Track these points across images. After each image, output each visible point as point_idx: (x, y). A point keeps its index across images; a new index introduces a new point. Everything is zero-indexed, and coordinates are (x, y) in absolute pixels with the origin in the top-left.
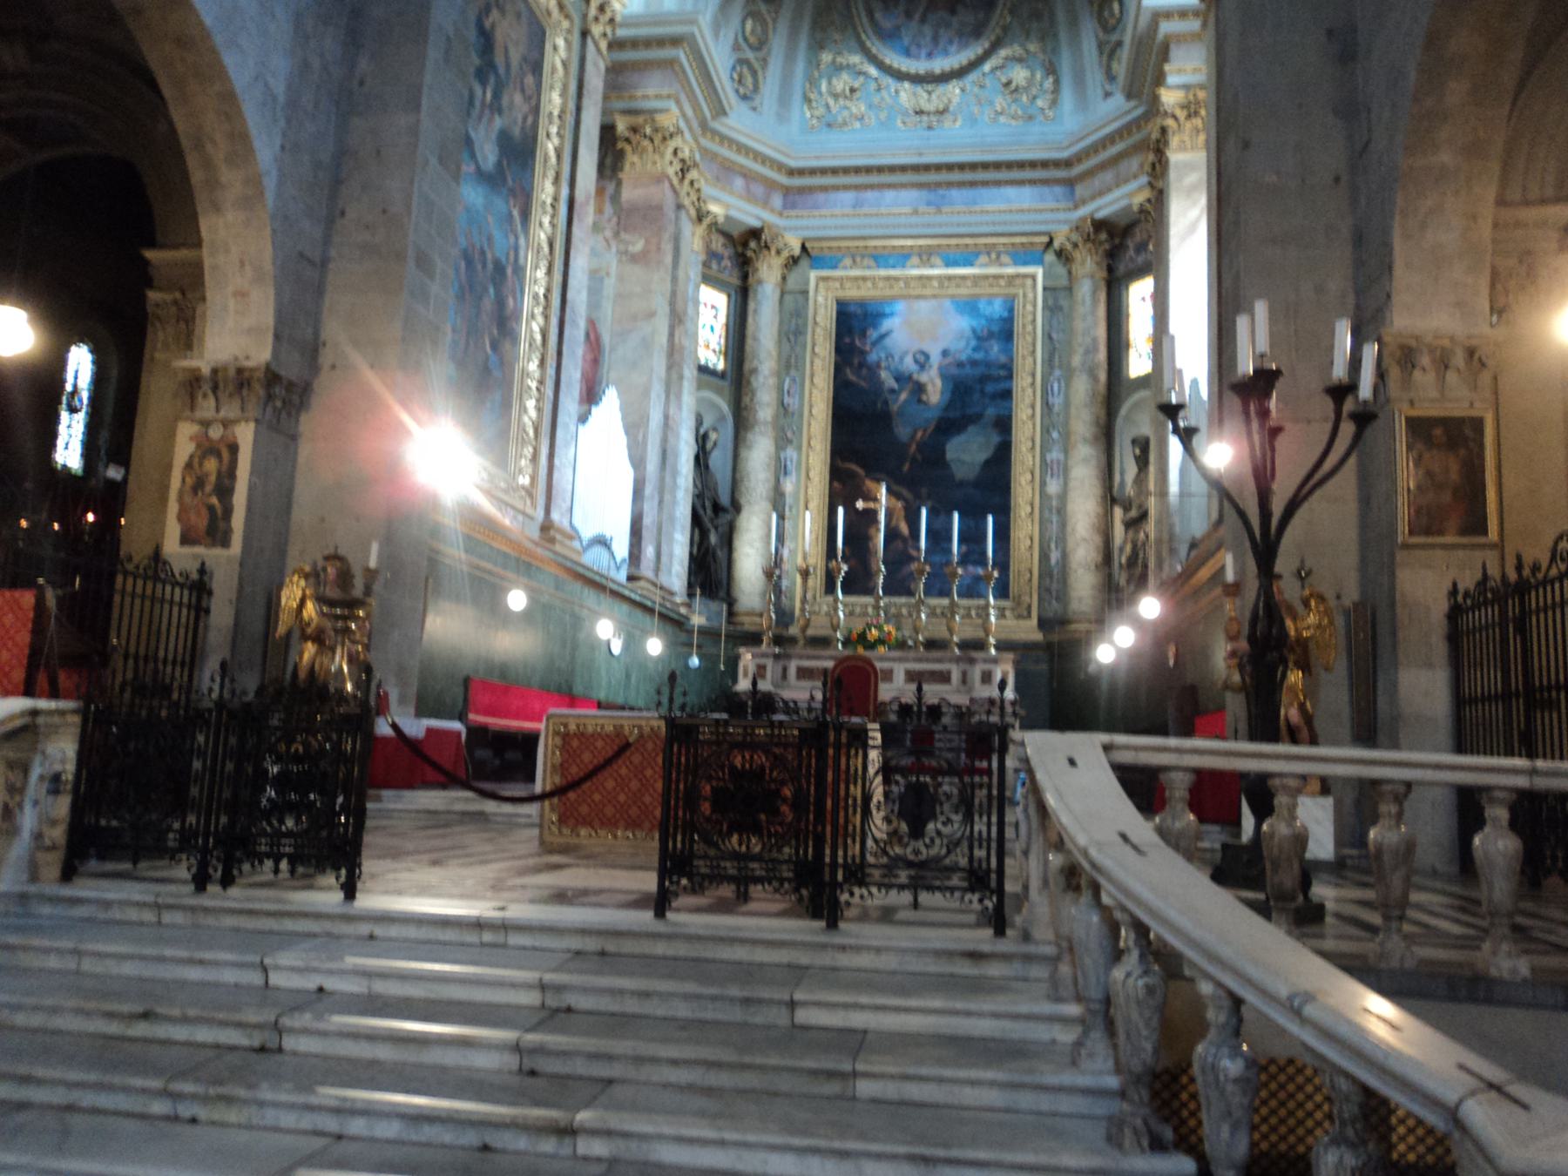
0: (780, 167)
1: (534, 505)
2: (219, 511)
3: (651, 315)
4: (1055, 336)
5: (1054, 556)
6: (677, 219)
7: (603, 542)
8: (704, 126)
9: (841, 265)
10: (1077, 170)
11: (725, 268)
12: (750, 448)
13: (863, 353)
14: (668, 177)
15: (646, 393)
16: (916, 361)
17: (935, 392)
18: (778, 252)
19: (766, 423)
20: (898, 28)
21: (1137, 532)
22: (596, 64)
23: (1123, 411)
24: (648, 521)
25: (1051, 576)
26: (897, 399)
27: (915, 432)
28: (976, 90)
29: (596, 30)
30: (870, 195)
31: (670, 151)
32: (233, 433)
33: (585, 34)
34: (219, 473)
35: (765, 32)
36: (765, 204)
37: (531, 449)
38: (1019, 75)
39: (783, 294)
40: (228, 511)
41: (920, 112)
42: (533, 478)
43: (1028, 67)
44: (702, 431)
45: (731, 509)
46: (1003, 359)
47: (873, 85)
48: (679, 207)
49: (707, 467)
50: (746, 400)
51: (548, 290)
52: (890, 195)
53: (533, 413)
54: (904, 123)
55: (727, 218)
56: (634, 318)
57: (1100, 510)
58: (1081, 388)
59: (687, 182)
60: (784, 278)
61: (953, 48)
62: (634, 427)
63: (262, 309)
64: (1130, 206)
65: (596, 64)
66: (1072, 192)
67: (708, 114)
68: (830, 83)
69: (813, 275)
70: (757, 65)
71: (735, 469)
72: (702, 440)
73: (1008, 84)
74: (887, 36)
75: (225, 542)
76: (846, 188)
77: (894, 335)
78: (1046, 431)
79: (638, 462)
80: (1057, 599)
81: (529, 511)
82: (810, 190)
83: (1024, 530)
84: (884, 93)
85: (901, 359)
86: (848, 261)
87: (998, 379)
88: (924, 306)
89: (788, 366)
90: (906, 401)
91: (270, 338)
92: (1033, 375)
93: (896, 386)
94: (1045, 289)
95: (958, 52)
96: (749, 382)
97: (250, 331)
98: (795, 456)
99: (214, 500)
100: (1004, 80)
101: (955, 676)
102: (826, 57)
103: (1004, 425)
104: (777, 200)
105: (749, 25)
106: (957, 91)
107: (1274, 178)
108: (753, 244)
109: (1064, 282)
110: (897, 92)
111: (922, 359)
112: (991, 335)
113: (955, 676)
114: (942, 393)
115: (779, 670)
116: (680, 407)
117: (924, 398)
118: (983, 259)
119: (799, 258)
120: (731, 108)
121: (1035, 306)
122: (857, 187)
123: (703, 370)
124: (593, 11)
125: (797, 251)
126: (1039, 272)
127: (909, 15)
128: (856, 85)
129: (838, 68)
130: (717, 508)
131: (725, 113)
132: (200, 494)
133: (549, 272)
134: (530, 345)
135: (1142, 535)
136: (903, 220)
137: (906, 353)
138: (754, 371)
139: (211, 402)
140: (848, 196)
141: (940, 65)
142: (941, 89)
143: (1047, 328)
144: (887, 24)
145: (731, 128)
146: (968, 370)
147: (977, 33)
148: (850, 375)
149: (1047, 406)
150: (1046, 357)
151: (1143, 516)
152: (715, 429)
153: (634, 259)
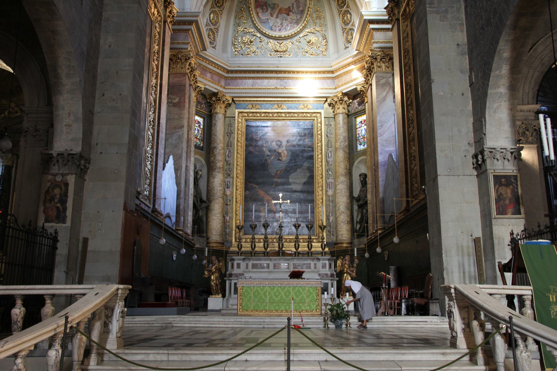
0: (224, 69)
1: (150, 202)
2: (61, 209)
3: (183, 127)
4: (328, 135)
5: (331, 219)
6: (190, 89)
7: (168, 216)
8: (197, 54)
9: (247, 108)
11: (203, 107)
12: (214, 178)
14: (187, 73)
15: (180, 157)
16: (277, 145)
18: (223, 102)
19: (220, 168)
20: (268, 19)
21: (363, 209)
22: (168, 34)
23: (355, 164)
24: (182, 207)
25: (330, 226)
26: (270, 159)
27: (278, 171)
28: (297, 43)
29: (169, 20)
30: (258, 81)
31: (188, 64)
32: (66, 179)
33: (165, 22)
34: (61, 195)
35: (218, 18)
36: (218, 83)
37: (149, 181)
38: (313, 38)
39: (225, 117)
40: (65, 209)
42: (150, 192)
43: (317, 36)
44: (196, 170)
45: (207, 202)
46: (310, 144)
47: (258, 40)
48: (190, 85)
49: (198, 185)
50: (212, 159)
51: (154, 119)
52: (266, 82)
53: (149, 167)
54: (271, 55)
55: (205, 88)
56: (175, 128)
57: (348, 201)
58: (341, 155)
59: (192, 76)
60: (226, 112)
61: (289, 28)
62: (177, 169)
63: (78, 131)
64: (356, 89)
65: (168, 34)
66: (334, 83)
67: (199, 50)
69: (237, 110)
70: (215, 31)
71: (208, 186)
72: (196, 173)
73: (309, 42)
74: (263, 22)
75: (64, 222)
77: (268, 134)
78: (327, 171)
79: (178, 184)
80: (333, 235)
81: (149, 205)
82: (236, 78)
84: (263, 43)
86: (250, 106)
87: (309, 151)
89: (228, 146)
90: (273, 159)
91: (81, 142)
92: (322, 150)
93: (269, 154)
94: (325, 117)
95: (290, 29)
96: (213, 152)
97: (72, 140)
99: (59, 205)
100: (308, 40)
101: (312, 266)
102: (241, 29)
103: (311, 170)
104: (223, 83)
105: (212, 16)
106: (290, 43)
107: (442, 93)
108: (214, 99)
109: (332, 115)
110: (268, 43)
111: (279, 144)
112: (305, 135)
113: (312, 266)
114: (287, 156)
115: (245, 265)
116: (190, 163)
117: (280, 158)
119: (231, 103)
120: (208, 48)
121: (321, 124)
122: (253, 78)
123: (197, 147)
124: (168, 14)
125: (231, 101)
127: (272, 15)
128: (252, 40)
130: (202, 201)
131: (206, 50)
132: (53, 203)
133: (154, 113)
134: (148, 141)
135: (364, 211)
137: (273, 141)
138: (215, 147)
139: (57, 167)
140: (250, 81)
141: (283, 34)
142: (285, 42)
143: (326, 133)
144: (263, 17)
145: (207, 55)
146: (297, 148)
147: (297, 23)
148: (251, 149)
149: (327, 162)
150: (326, 143)
151: (366, 203)
152: (201, 171)
153: (175, 105)
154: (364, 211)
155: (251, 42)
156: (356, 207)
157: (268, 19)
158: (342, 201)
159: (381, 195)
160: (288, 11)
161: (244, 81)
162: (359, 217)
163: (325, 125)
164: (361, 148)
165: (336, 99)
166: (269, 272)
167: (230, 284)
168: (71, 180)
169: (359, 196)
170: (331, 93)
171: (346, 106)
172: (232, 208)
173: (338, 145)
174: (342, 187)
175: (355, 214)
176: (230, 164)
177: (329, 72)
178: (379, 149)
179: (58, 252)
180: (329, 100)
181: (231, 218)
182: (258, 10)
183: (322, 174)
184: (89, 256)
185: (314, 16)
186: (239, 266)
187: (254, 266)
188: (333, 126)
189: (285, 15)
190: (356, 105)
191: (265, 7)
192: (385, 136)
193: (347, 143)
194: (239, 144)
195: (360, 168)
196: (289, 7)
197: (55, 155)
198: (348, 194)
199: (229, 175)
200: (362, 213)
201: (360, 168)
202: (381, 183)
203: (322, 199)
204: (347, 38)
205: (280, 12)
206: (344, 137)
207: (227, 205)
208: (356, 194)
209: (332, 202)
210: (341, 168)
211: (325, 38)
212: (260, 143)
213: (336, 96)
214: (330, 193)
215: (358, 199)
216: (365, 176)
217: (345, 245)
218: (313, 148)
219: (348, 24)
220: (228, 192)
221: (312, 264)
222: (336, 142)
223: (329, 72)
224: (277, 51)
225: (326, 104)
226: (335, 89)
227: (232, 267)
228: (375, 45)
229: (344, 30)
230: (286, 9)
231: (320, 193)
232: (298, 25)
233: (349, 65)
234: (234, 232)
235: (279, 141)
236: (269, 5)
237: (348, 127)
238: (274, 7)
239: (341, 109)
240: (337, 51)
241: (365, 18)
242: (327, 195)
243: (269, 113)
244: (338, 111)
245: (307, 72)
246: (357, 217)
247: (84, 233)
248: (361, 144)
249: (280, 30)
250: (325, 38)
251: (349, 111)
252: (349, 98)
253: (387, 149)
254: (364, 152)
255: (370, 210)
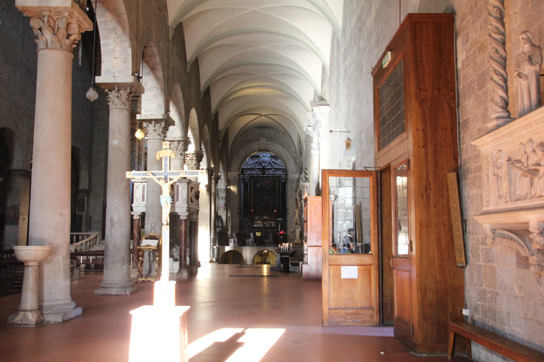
40: (84, 208)
63: (87, 182)
75: (84, 211)
99: (82, 206)
168: (86, 198)
179: (83, 221)
184: (92, 222)
197: (80, 190)
247: (90, 214)
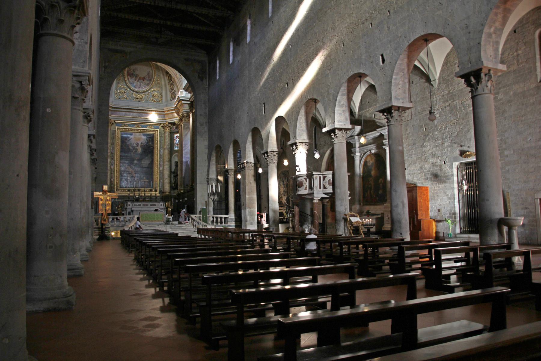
10: (165, 113)
13: (126, 143)
16: (136, 145)
17: (140, 150)
23: (173, 156)
28: (148, 95)
30: (128, 113)
41: (137, 99)
46: (152, 145)
47: (128, 92)
52: (132, 114)
57: (169, 173)
58: (166, 152)
61: (143, 87)
64: (175, 122)
66: (164, 116)
68: (120, 91)
73: (153, 95)
74: (130, 83)
76: (123, 111)
78: (160, 159)
82: (117, 111)
83: (156, 176)
85: (134, 144)
86: (123, 125)
88: (137, 134)
92: (158, 148)
95: (144, 88)
98: (114, 161)
101: (157, 205)
109: (163, 132)
118: (148, 127)
125: (114, 122)
126: (159, 130)
127: (135, 80)
129: (121, 88)
136: (134, 119)
140: (124, 113)
141: (141, 90)
142: (141, 94)
144: (131, 81)
147: (148, 85)
149: (160, 154)
151: (177, 175)
154: (176, 179)
155: (124, 93)
156: (172, 176)
157: (133, 82)
158: (167, 173)
159: (183, 175)
160: (144, 79)
161: (121, 112)
162: (174, 181)
163: (159, 136)
164: (176, 149)
165: (165, 125)
166: (141, 207)
167: (126, 212)
169: (174, 171)
170: (163, 122)
171: (170, 129)
172: (114, 175)
173: (165, 147)
174: (167, 167)
175: (172, 179)
176: (113, 154)
177: (162, 111)
178: (183, 156)
180: (162, 125)
181: (114, 180)
182: (129, 77)
183: (157, 160)
185: (156, 82)
186: (129, 205)
187: (135, 205)
188: (163, 137)
189: (142, 81)
190: (175, 128)
191: (132, 76)
192: (186, 150)
193: (169, 146)
194: (118, 144)
195: (175, 159)
196: (144, 77)
198: (169, 170)
199: (113, 159)
200: (175, 179)
201: (175, 159)
202: (183, 170)
203: (157, 172)
204: (172, 96)
205: (140, 79)
206: (168, 144)
207: (112, 173)
208: (173, 170)
209: (162, 173)
210: (167, 158)
211: (161, 94)
212: (128, 143)
213: (165, 123)
214: (161, 169)
215: (174, 173)
216: (177, 162)
217: (167, 193)
218: (153, 147)
219: (173, 90)
220: (112, 167)
221: (157, 204)
222: (164, 145)
223: (162, 111)
224: (137, 99)
225: (160, 126)
226: (165, 120)
227: (127, 205)
228: (184, 110)
229: (170, 92)
230: (143, 78)
231: (156, 169)
232: (148, 86)
233: (172, 110)
234: (115, 186)
235: (137, 143)
236: (134, 75)
237: (170, 138)
238: (136, 76)
239: (167, 130)
240: (167, 101)
241: (180, 99)
242: (160, 170)
243: (132, 129)
244: (166, 131)
245: (152, 111)
246: (173, 181)
248: (176, 147)
249: (139, 88)
250: (161, 94)
251: (171, 131)
252: (171, 125)
253: (187, 156)
254: (177, 151)
255: (179, 179)
